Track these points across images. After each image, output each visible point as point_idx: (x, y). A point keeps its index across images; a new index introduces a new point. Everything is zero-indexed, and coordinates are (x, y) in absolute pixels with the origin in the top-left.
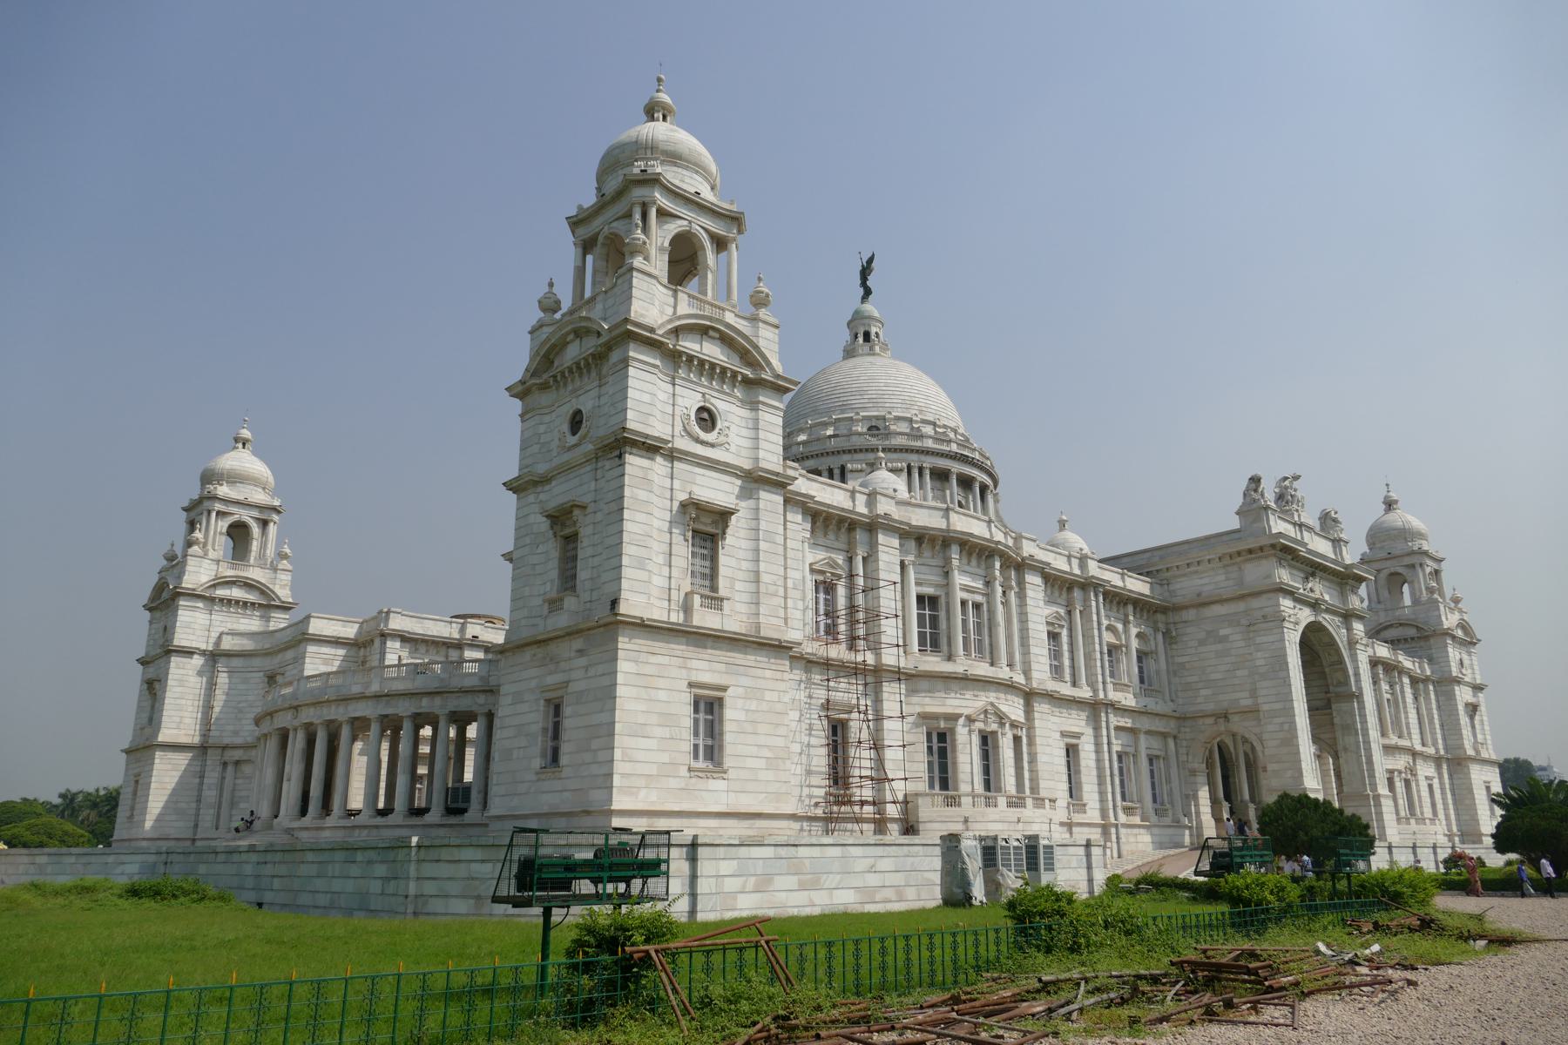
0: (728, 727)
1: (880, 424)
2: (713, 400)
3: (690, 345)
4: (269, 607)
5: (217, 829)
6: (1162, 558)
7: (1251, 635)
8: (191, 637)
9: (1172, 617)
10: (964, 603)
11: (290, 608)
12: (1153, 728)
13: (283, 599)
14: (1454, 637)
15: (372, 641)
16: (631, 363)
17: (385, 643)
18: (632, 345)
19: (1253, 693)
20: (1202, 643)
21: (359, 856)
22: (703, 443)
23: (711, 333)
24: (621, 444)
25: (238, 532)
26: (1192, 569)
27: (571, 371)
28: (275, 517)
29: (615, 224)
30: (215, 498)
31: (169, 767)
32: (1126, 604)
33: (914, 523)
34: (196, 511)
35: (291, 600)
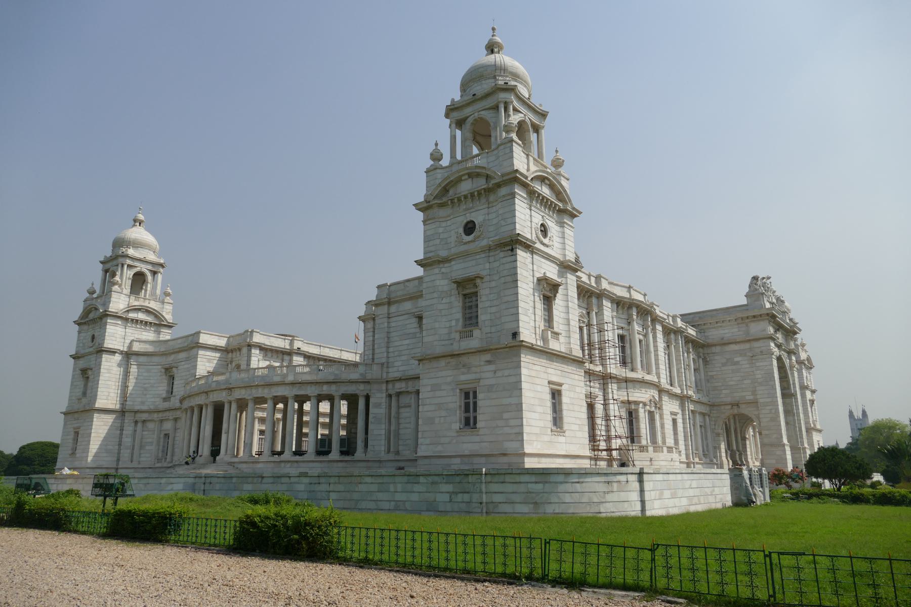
0: (564, 407)
2: (547, 221)
4: (160, 325)
5: (132, 462)
6: (700, 318)
7: (754, 361)
8: (114, 342)
11: (172, 327)
13: (169, 321)
14: (805, 365)
15: (240, 349)
16: (517, 196)
17: (251, 351)
18: (516, 186)
19: (754, 393)
20: (724, 365)
21: (422, 479)
23: (547, 181)
25: (139, 280)
26: (719, 325)
27: (466, 197)
28: (161, 270)
29: (482, 113)
31: (102, 423)
35: (171, 321)
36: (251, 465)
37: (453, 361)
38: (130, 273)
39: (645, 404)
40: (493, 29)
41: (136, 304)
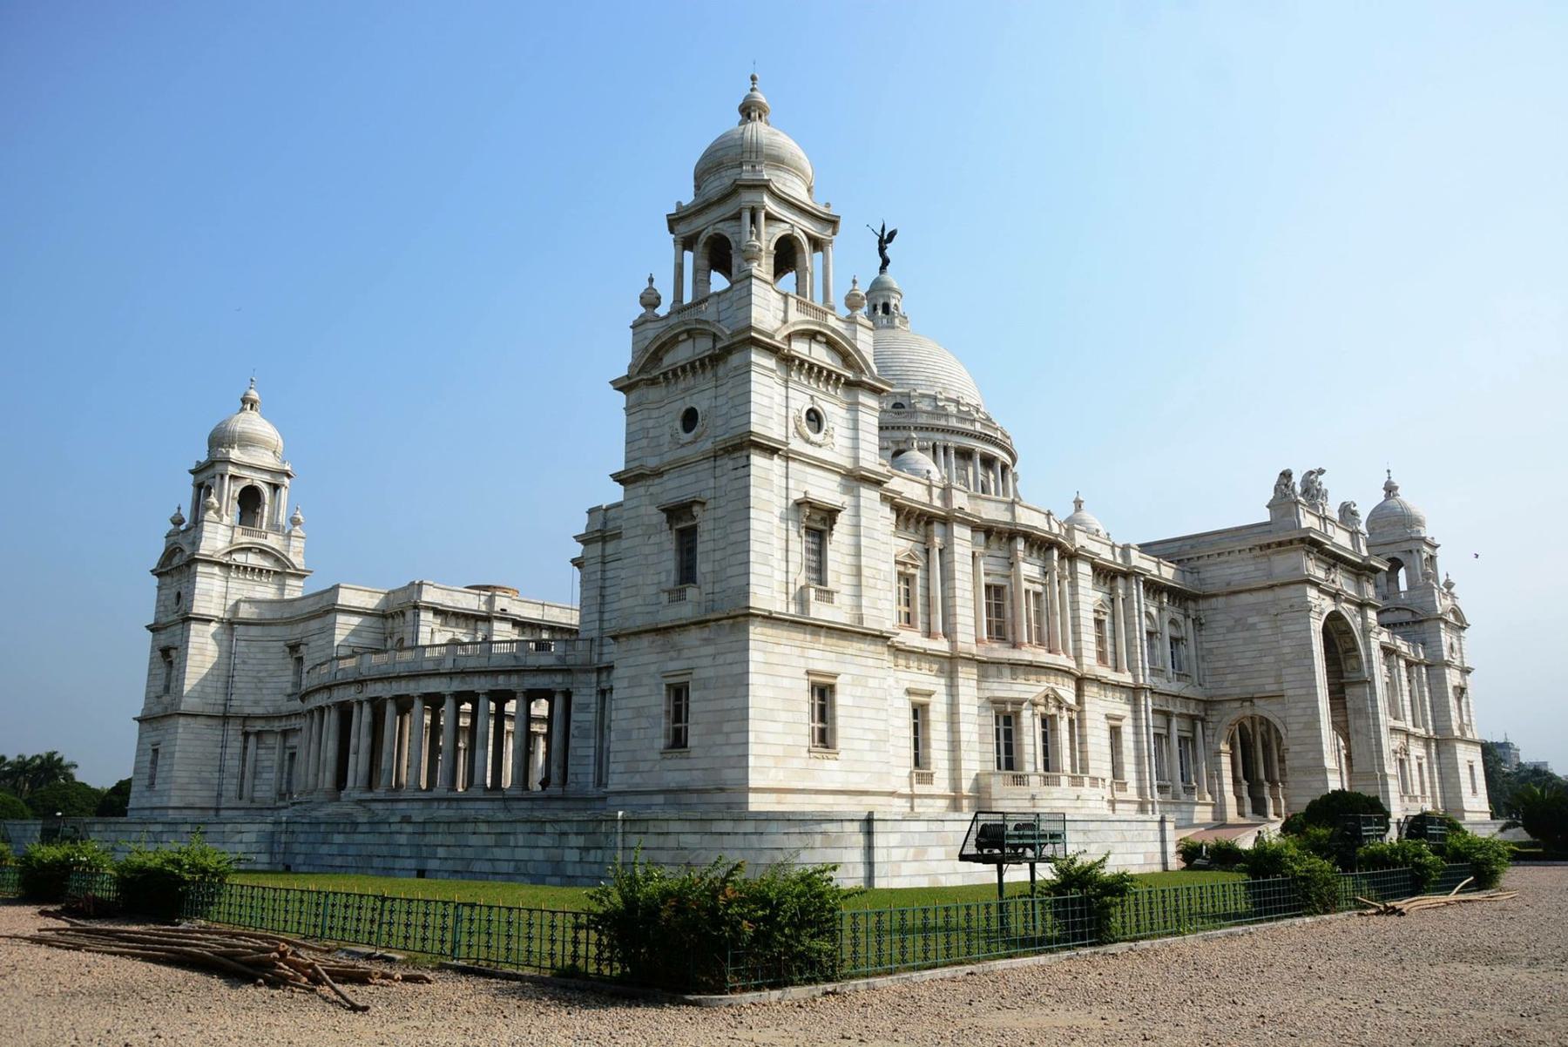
0: (839, 711)
1: (905, 402)
2: (820, 402)
3: (800, 348)
6: (1192, 547)
7: (1279, 624)
8: (208, 605)
9: (1203, 605)
10: (1027, 591)
11: (304, 576)
12: (1185, 711)
13: (298, 567)
14: (1446, 622)
15: (403, 614)
16: (753, 368)
17: (418, 616)
18: (753, 350)
20: (1230, 630)
21: (548, 828)
22: (812, 443)
23: (819, 338)
24: (745, 444)
25: (250, 500)
26: (1223, 558)
27: (683, 368)
28: (286, 481)
29: (720, 226)
30: (228, 462)
31: (191, 736)
32: (1161, 592)
33: (985, 517)
34: (206, 477)
35: (303, 568)
36: (389, 805)
37: (659, 639)
38: (233, 490)
39: (1034, 704)
40: (753, 78)
41: (243, 541)
